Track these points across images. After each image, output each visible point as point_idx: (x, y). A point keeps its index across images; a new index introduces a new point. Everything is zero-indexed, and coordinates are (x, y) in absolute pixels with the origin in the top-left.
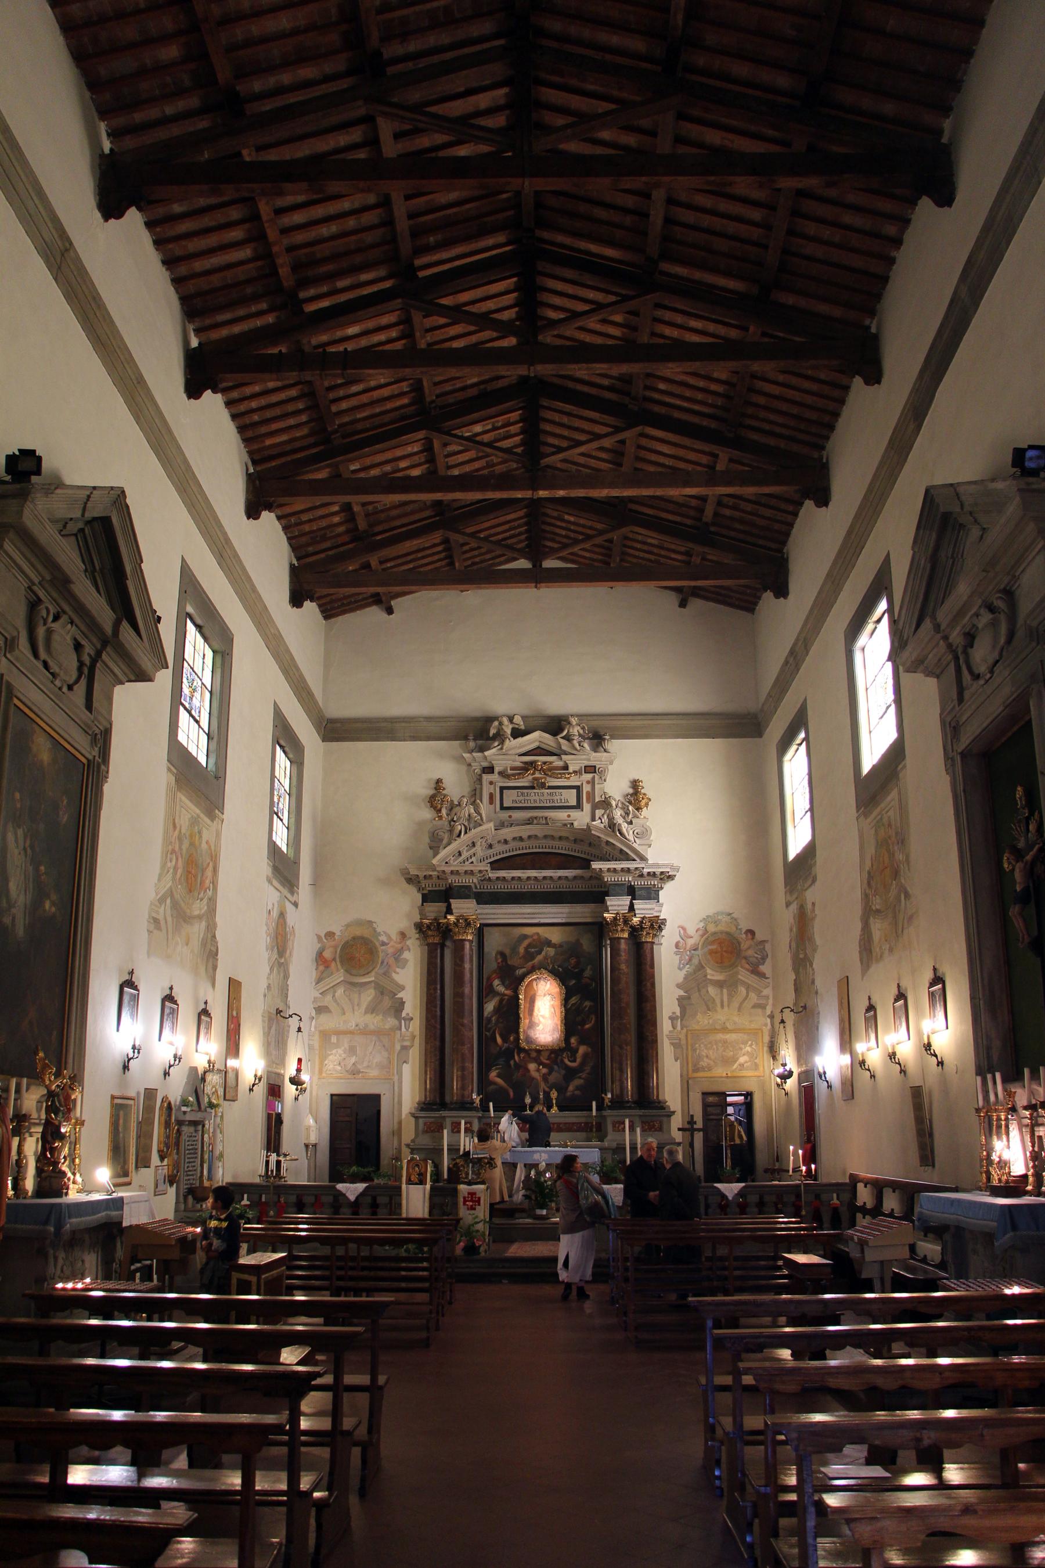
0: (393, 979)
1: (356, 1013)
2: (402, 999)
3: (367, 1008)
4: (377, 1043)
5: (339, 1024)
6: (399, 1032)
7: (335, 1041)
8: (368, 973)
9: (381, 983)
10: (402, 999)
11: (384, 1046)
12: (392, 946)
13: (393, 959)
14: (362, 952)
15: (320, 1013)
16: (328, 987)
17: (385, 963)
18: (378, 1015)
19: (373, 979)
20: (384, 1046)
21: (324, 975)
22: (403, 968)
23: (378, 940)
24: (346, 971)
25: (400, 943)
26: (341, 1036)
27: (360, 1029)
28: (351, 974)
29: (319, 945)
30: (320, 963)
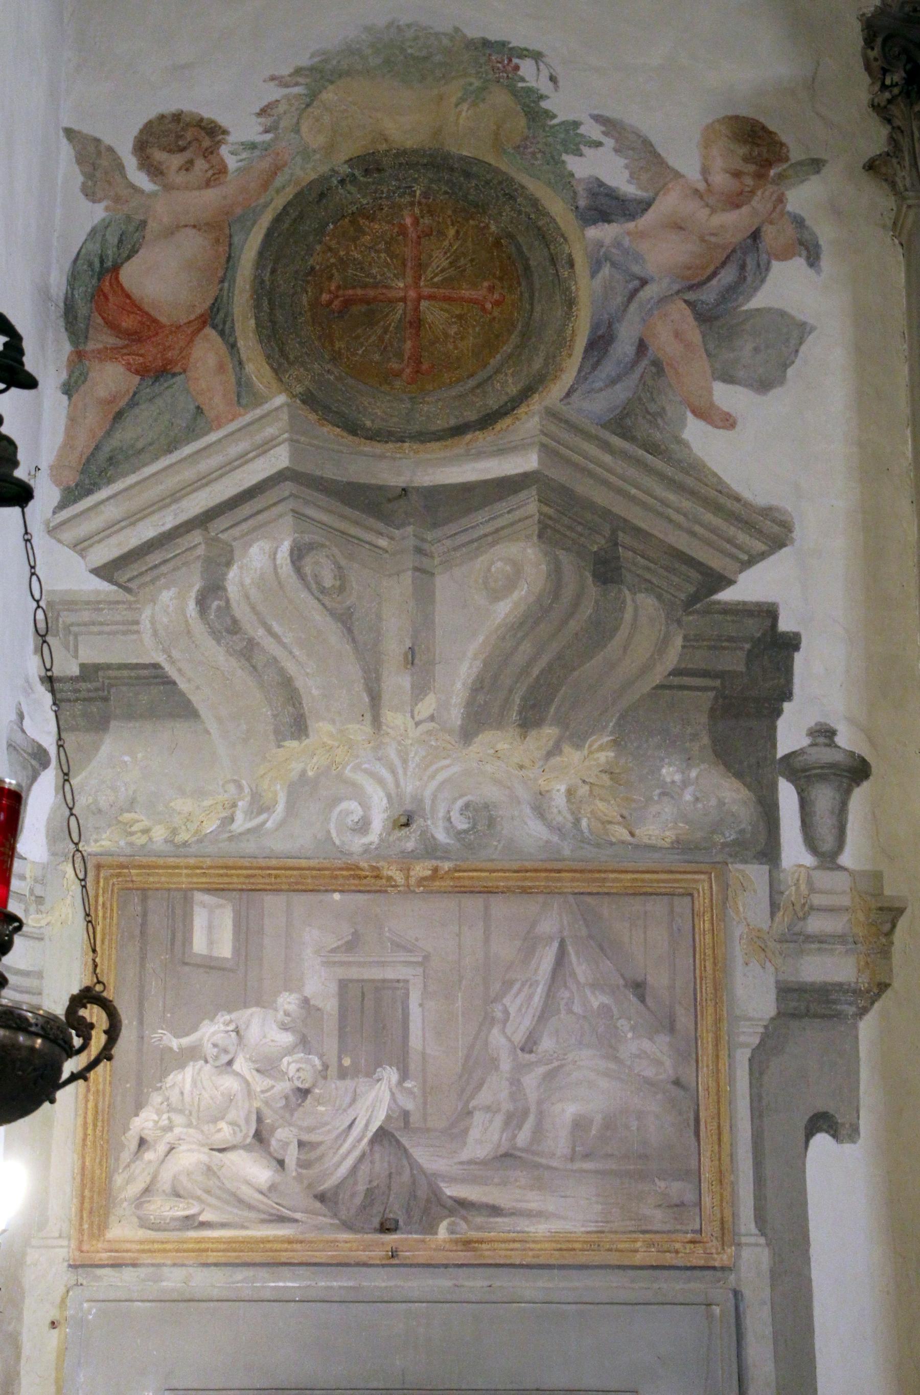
0: (696, 468)
1: (394, 719)
2: (770, 613)
3: (478, 687)
4: (581, 969)
5: (259, 806)
6: (757, 873)
7: (225, 950)
8: (487, 421)
9: (584, 488)
10: (770, 613)
11: (639, 988)
12: (678, 226)
13: (679, 312)
14: (439, 260)
15: (100, 724)
16: (168, 520)
17: (624, 347)
18: (578, 740)
19: (529, 462)
20: (639, 988)
21: (126, 434)
22: (763, 385)
23: (565, 181)
24: (309, 400)
25: (735, 201)
26: (273, 903)
27: (431, 849)
28: (353, 429)
29: (98, 213)
30: (103, 339)
